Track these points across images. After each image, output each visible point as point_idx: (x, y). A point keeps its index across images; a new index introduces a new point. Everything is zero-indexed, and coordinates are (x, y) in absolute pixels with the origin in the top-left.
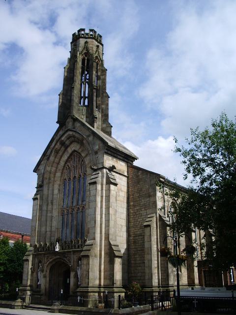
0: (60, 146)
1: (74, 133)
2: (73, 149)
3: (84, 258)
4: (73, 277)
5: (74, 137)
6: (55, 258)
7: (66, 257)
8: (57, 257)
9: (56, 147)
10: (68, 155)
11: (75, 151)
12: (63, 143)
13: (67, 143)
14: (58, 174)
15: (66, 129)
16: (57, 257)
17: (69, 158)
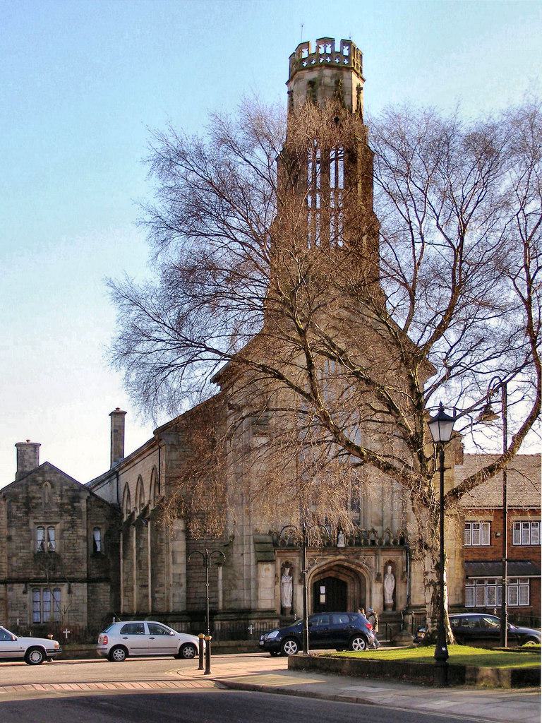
4: (378, 592)
6: (334, 558)
8: (338, 558)
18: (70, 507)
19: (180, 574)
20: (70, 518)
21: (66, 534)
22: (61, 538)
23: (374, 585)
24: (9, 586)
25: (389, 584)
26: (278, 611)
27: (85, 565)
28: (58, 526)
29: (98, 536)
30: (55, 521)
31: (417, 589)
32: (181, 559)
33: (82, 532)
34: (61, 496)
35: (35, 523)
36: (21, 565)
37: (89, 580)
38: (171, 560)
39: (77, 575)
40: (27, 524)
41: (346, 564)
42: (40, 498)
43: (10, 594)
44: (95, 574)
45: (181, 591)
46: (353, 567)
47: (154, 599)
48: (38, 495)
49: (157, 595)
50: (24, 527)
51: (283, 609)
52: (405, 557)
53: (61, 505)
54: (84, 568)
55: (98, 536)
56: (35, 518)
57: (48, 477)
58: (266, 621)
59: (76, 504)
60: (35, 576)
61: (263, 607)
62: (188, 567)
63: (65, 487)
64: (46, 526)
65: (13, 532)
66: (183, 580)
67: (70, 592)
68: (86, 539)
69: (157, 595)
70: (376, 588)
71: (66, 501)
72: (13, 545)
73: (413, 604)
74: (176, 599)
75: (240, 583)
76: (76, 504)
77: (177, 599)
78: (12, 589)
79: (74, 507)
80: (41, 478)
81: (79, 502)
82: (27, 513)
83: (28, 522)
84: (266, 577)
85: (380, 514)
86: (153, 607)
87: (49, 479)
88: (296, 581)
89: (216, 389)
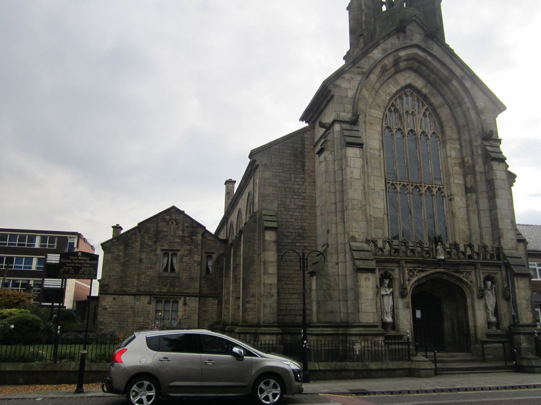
0: (392, 65)
1: (429, 58)
2: (408, 82)
3: (519, 278)
4: (482, 308)
5: (422, 62)
6: (434, 270)
7: (461, 273)
8: (438, 270)
9: (386, 62)
10: (398, 88)
11: (409, 86)
12: (396, 62)
13: (402, 65)
14: (378, 113)
15: (409, 43)
16: (438, 270)
17: (398, 92)
18: (189, 239)
19: (271, 284)
20: (188, 247)
21: (185, 259)
22: (181, 261)
23: (476, 300)
24: (137, 297)
25: (491, 300)
26: (379, 324)
27: (198, 283)
28: (179, 253)
29: (210, 263)
30: (176, 249)
31: (524, 306)
32: (272, 269)
33: (197, 258)
34: (183, 231)
35: (162, 250)
36: (148, 281)
37: (201, 296)
38: (262, 271)
39: (191, 291)
40: (156, 250)
41: (445, 278)
42: (167, 231)
43: (137, 303)
44: (206, 291)
45: (272, 302)
46: (453, 281)
47: (245, 310)
48: (166, 230)
49: (248, 305)
50: (153, 253)
51: (385, 325)
52: (504, 272)
53: (182, 238)
54: (197, 286)
55: (210, 263)
56: (162, 246)
57: (174, 217)
58: (370, 337)
59: (194, 237)
60: (158, 290)
61: (364, 321)
62: (279, 279)
63: (186, 224)
64: (170, 253)
65: (144, 256)
66: (274, 291)
67: (185, 304)
68: (200, 263)
69: (248, 305)
70: (479, 305)
71: (186, 235)
72: (143, 266)
73: (521, 322)
74: (266, 310)
75: (335, 294)
76: (194, 237)
77: (267, 310)
78: (139, 300)
79: (192, 239)
80: (168, 217)
81: (196, 236)
82: (156, 242)
83: (156, 249)
84: (367, 287)
85: (467, 232)
86: (243, 317)
87: (174, 218)
88: (397, 294)
89: (304, 125)
